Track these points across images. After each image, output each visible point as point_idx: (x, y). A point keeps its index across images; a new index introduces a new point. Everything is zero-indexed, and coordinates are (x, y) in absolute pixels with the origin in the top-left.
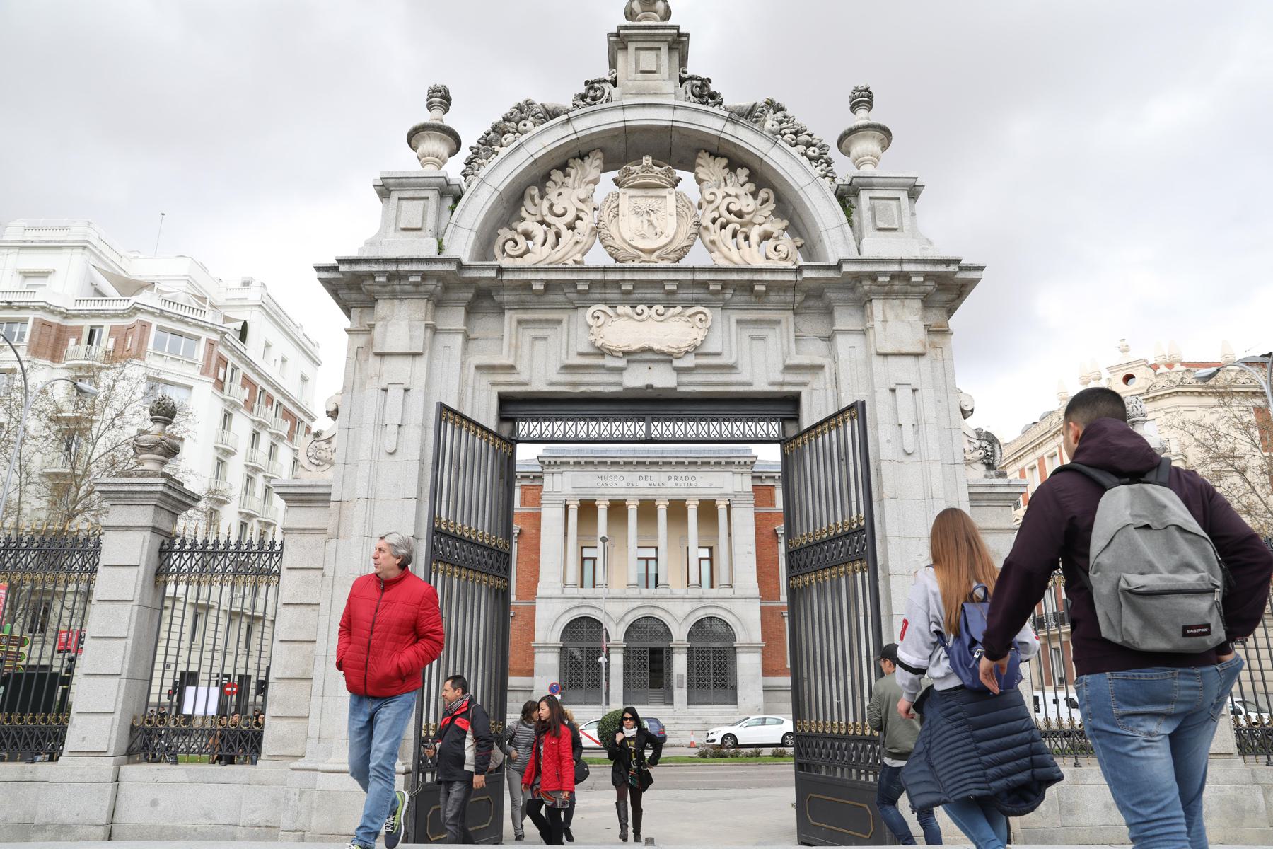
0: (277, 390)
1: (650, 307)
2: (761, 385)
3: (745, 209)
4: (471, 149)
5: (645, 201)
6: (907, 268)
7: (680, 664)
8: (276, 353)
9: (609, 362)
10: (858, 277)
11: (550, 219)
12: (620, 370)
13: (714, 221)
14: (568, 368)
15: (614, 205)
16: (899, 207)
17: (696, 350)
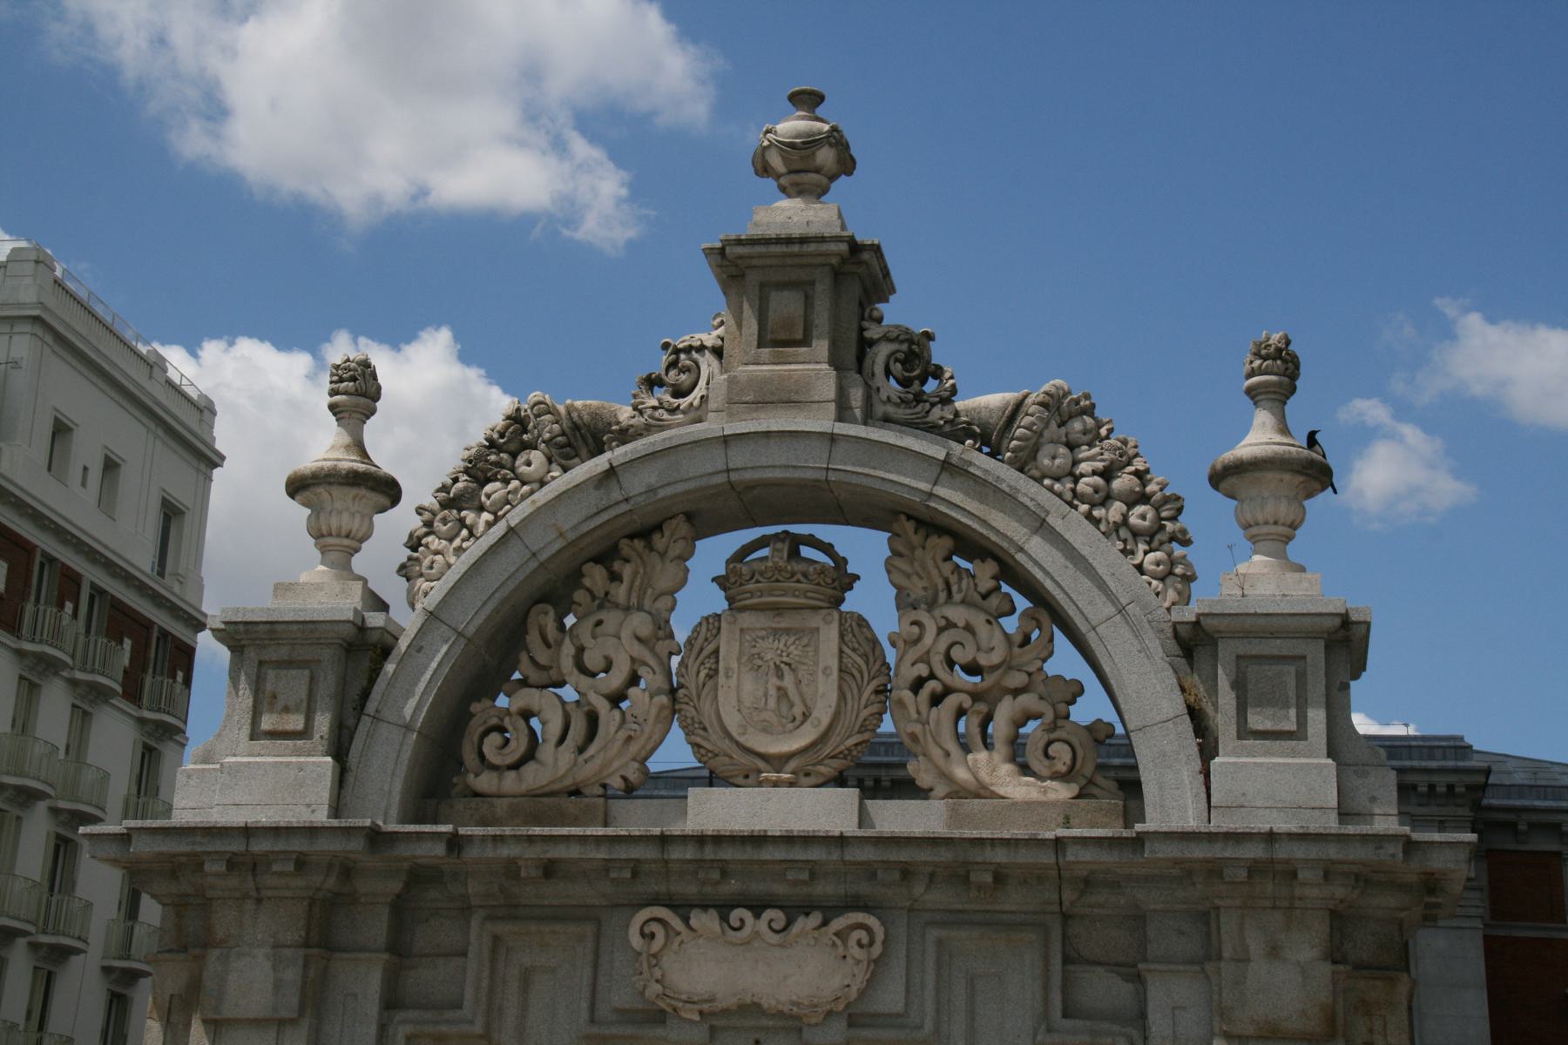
1: (757, 916)
3: (983, 660)
4: (420, 510)
8: (86, 451)
13: (917, 685)
15: (710, 648)
16: (1301, 677)
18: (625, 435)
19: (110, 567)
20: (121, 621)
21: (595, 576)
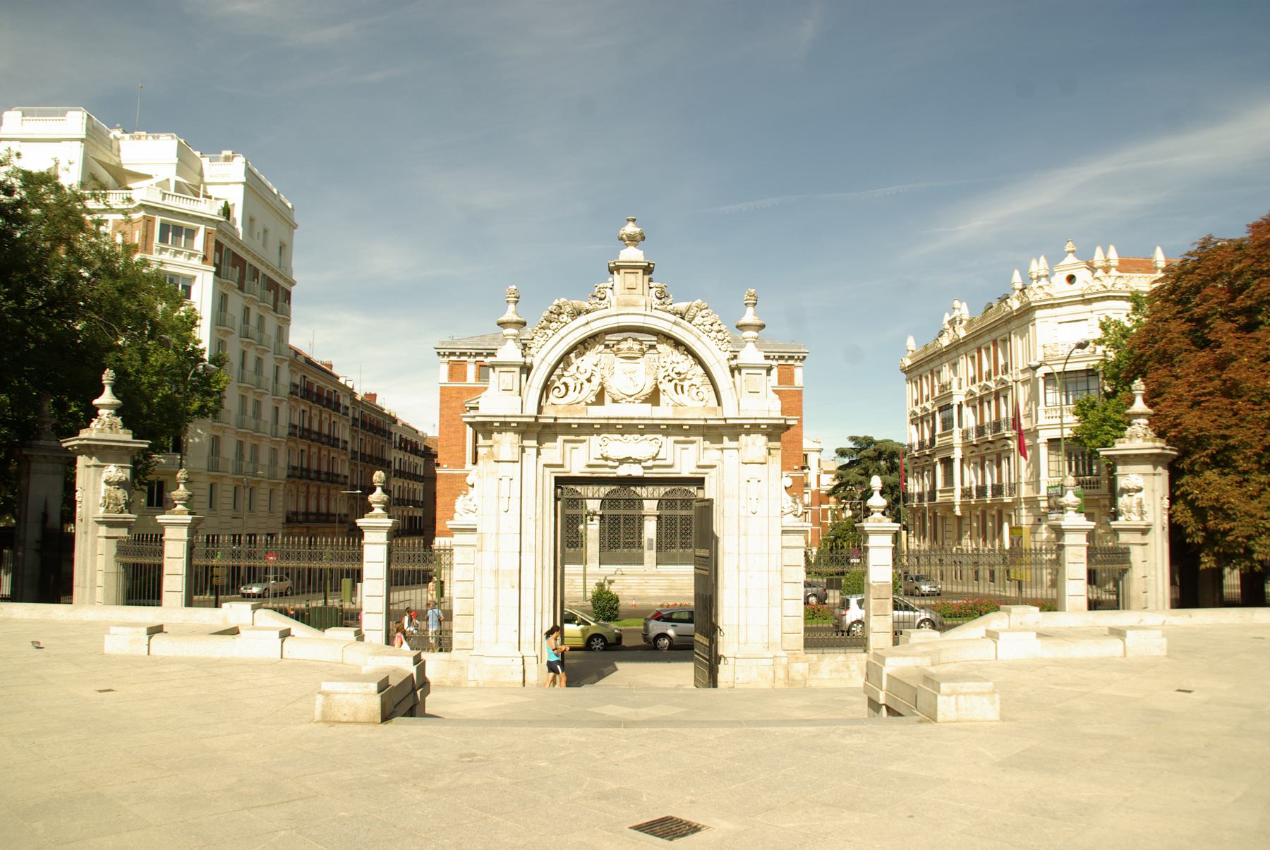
0: (262, 263)
2: (685, 474)
5: (629, 365)
6: (758, 422)
7: (650, 529)
8: (259, 229)
9: (610, 463)
10: (735, 425)
11: (578, 375)
12: (615, 467)
14: (589, 466)
17: (654, 459)
18: (588, 312)
19: (268, 267)
20: (271, 285)
21: (581, 347)
